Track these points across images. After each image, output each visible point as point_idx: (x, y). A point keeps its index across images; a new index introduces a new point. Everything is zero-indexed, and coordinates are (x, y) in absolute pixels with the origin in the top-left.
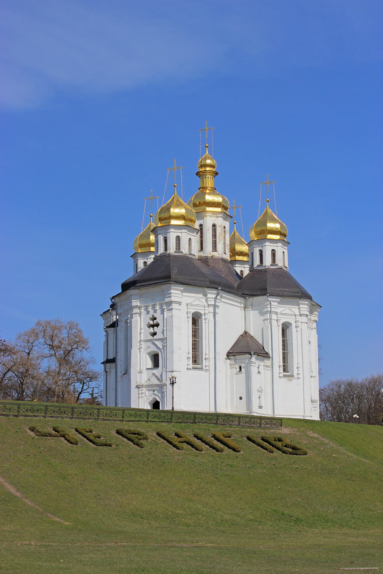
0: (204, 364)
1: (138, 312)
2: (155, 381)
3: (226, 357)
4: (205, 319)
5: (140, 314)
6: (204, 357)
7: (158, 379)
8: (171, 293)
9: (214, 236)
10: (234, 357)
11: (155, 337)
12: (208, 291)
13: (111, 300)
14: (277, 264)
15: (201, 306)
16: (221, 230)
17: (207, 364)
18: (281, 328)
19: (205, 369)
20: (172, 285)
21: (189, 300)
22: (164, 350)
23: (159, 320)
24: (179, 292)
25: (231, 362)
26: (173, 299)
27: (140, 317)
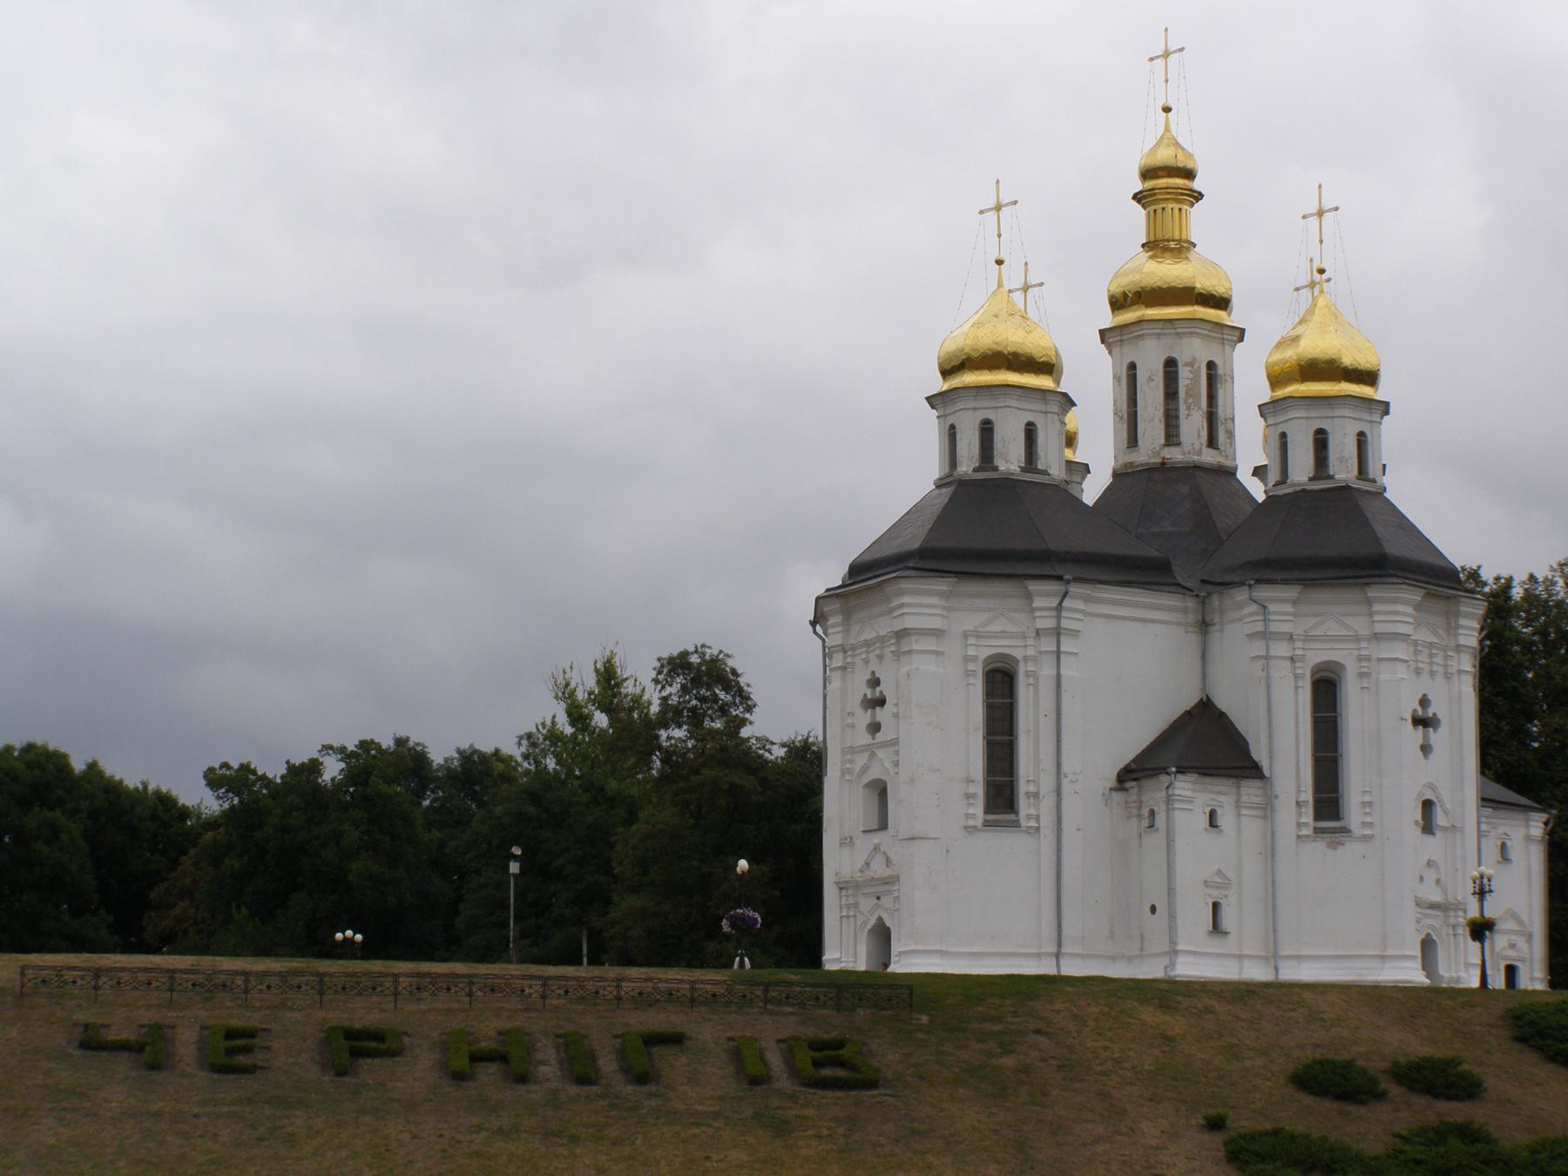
2: (879, 869)
3: (1112, 782)
9: (1171, 394)
10: (1133, 784)
11: (880, 737)
12: (1033, 586)
14: (1331, 473)
15: (1014, 636)
16: (1191, 376)
17: (1032, 811)
19: (1027, 827)
20: (902, 581)
21: (971, 621)
23: (886, 688)
24: (935, 600)
26: (910, 622)
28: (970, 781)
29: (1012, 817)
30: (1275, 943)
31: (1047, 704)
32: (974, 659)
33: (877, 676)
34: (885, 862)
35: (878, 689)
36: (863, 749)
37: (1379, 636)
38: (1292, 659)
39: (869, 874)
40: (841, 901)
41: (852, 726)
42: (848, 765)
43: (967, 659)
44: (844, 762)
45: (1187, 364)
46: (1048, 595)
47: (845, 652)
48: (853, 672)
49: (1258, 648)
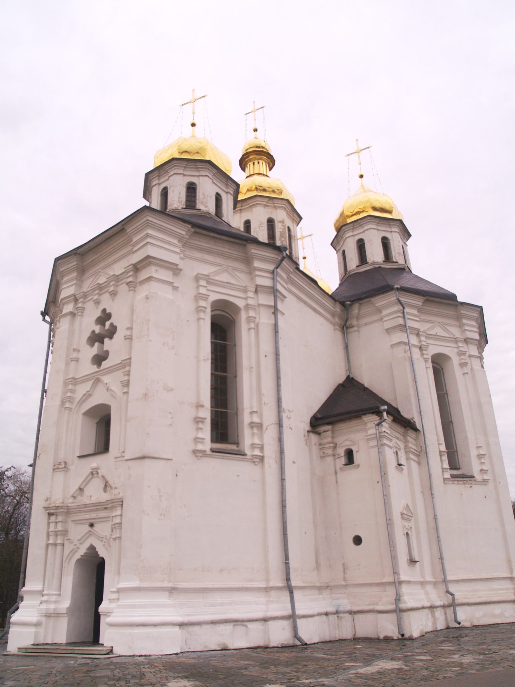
3: (308, 427)
10: (329, 427)
11: (105, 364)
13: (41, 317)
14: (395, 260)
16: (283, 228)
17: (257, 441)
18: (430, 365)
19: (253, 456)
24: (175, 241)
28: (199, 406)
29: (234, 447)
30: (443, 571)
31: (267, 346)
32: (205, 297)
33: (107, 312)
34: (103, 486)
35: (108, 324)
36: (85, 379)
37: (468, 340)
38: (420, 348)
39: (85, 500)
40: (48, 527)
41: (77, 360)
42: (69, 394)
43: (199, 297)
44: (64, 393)
45: (280, 222)
47: (76, 300)
48: (82, 316)
49: (399, 337)
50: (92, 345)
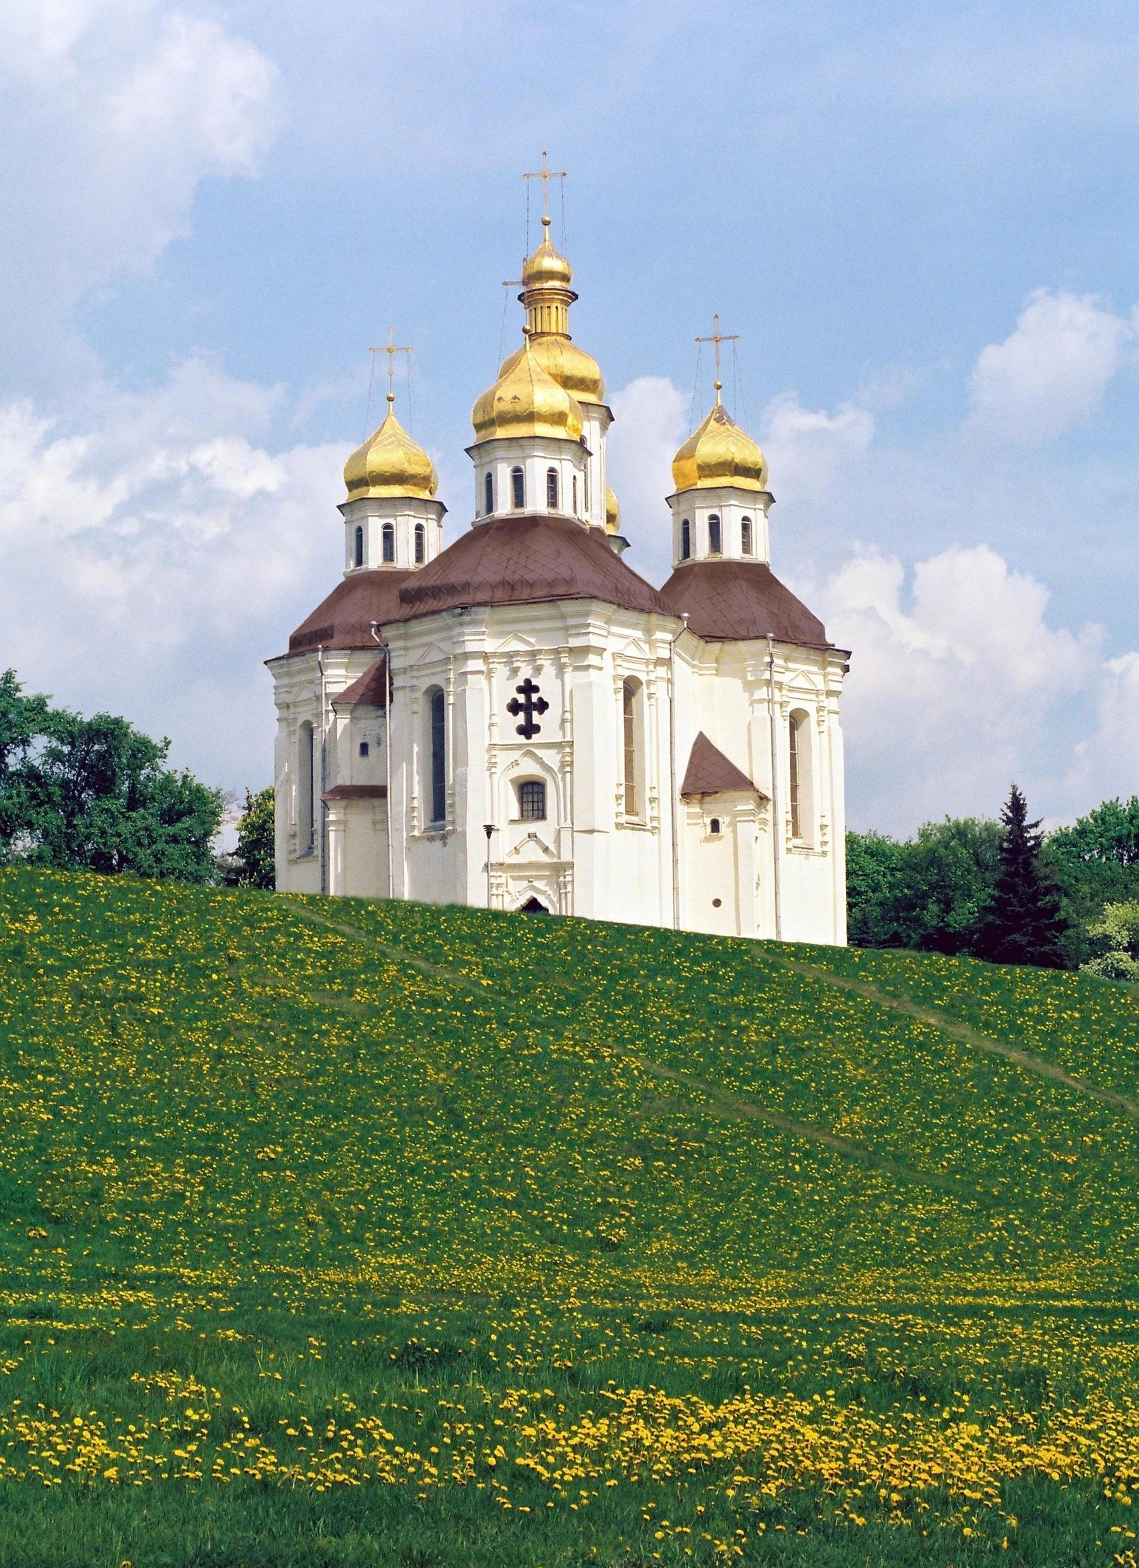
0: (649, 813)
1: (484, 668)
4: (650, 696)
5: (489, 674)
6: (648, 794)
7: (546, 850)
8: (588, 625)
11: (536, 738)
22: (564, 773)
25: (692, 810)
27: (490, 683)
35: (535, 697)
46: (664, 629)
49: (762, 693)
50: (515, 713)
